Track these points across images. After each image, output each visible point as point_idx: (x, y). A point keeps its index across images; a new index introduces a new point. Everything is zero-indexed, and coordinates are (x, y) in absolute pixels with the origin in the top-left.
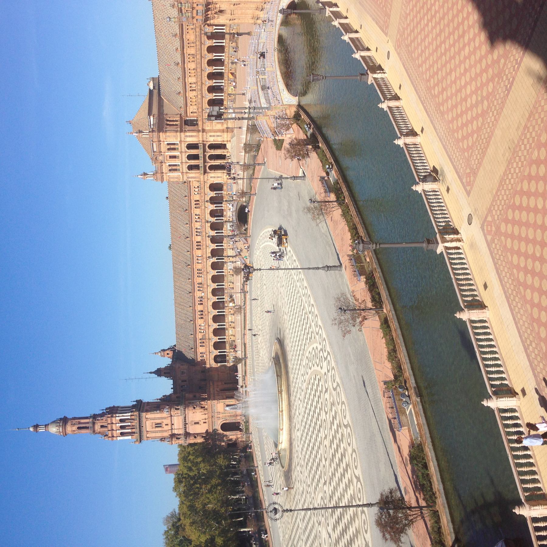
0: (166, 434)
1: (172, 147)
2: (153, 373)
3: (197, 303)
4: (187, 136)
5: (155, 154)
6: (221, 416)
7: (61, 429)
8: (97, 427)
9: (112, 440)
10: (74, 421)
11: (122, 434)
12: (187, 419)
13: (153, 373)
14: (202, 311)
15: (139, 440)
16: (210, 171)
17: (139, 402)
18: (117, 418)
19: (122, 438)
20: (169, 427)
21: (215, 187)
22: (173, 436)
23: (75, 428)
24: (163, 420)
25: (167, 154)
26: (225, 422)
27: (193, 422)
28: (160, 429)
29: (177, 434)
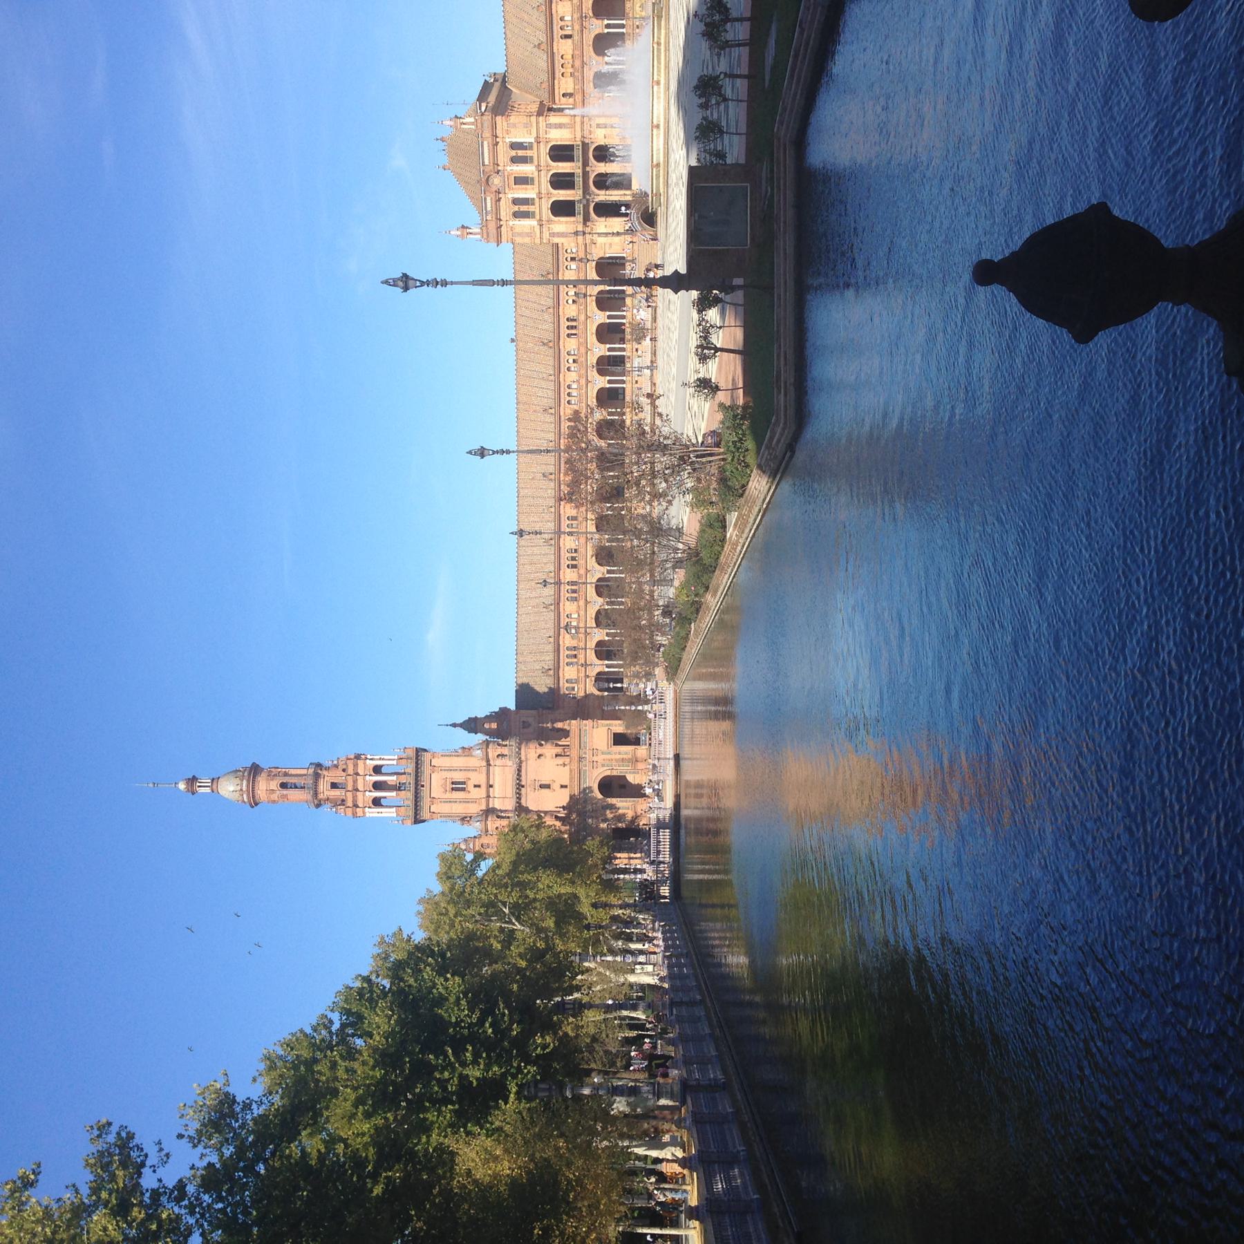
2: (461, 725)
3: (565, 563)
4: (549, 126)
6: (599, 758)
7: (245, 783)
9: (354, 815)
11: (377, 802)
12: (523, 773)
13: (461, 725)
19: (373, 813)
20: (482, 793)
22: (489, 812)
24: (470, 775)
25: (509, 168)
26: (608, 773)
27: (537, 784)
29: (502, 811)
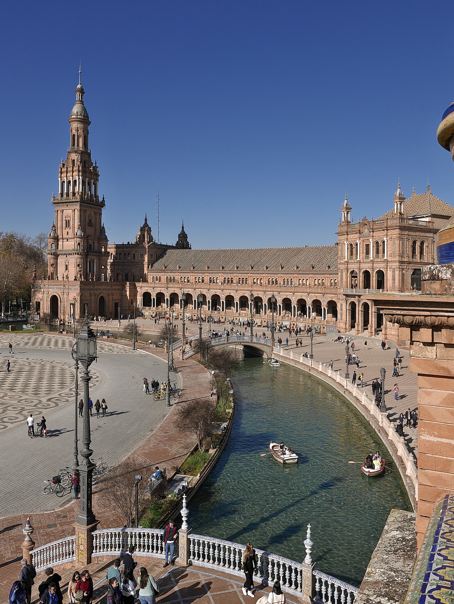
0: (59, 232)
1: (381, 248)
2: (146, 223)
4: (394, 272)
5: (371, 224)
7: (75, 117)
8: (74, 156)
10: (81, 131)
12: (71, 256)
13: (146, 223)
14: (203, 281)
15: (56, 201)
16: (348, 303)
17: (102, 204)
18: (77, 177)
21: (333, 308)
22: (56, 239)
23: (74, 132)
24: (71, 229)
25: (371, 240)
26: (59, 300)
28: (64, 226)
